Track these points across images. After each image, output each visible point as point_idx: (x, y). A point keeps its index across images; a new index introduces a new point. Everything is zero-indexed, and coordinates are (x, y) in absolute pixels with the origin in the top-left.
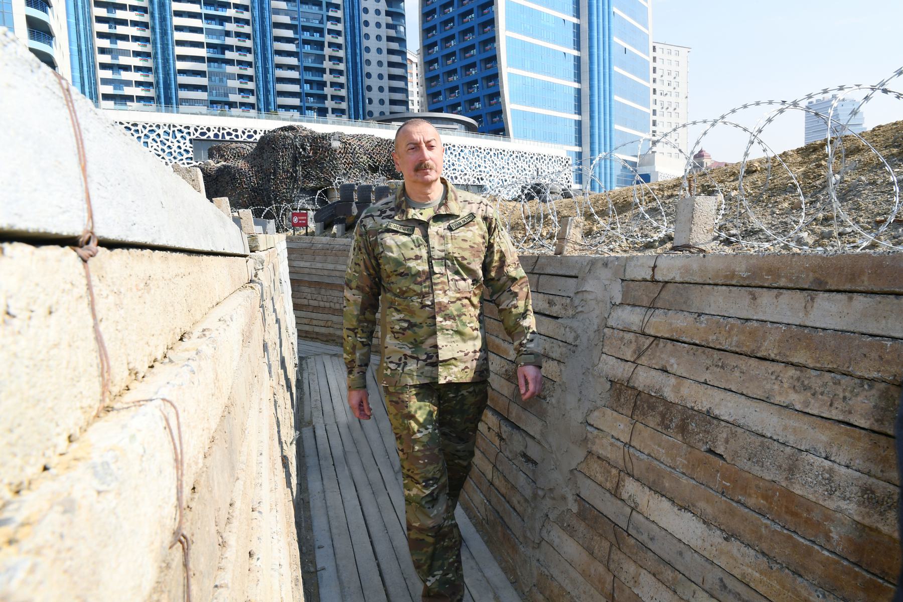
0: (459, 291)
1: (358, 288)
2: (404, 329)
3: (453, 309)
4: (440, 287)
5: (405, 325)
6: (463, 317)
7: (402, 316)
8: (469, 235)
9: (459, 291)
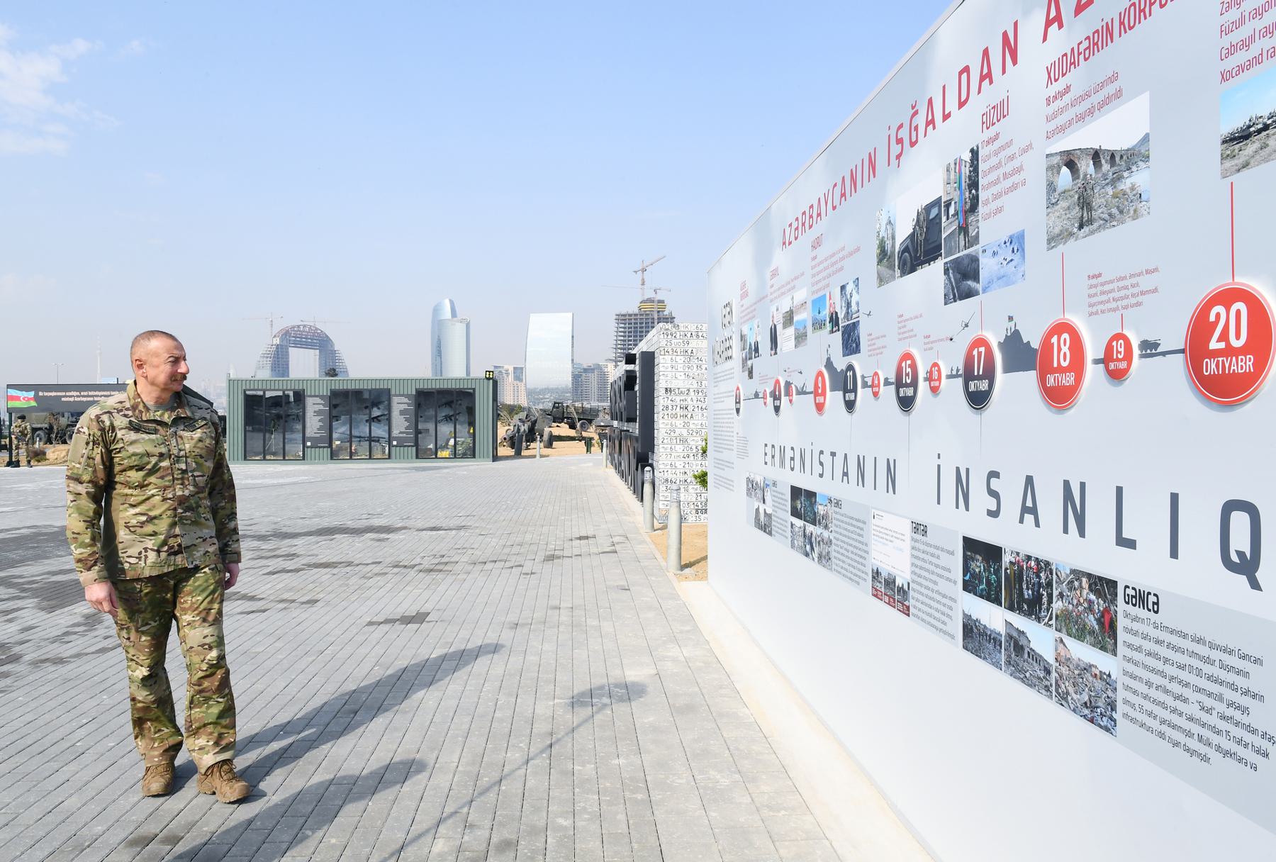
1: (89, 482)
2: (143, 523)
5: (144, 518)
7: (137, 510)
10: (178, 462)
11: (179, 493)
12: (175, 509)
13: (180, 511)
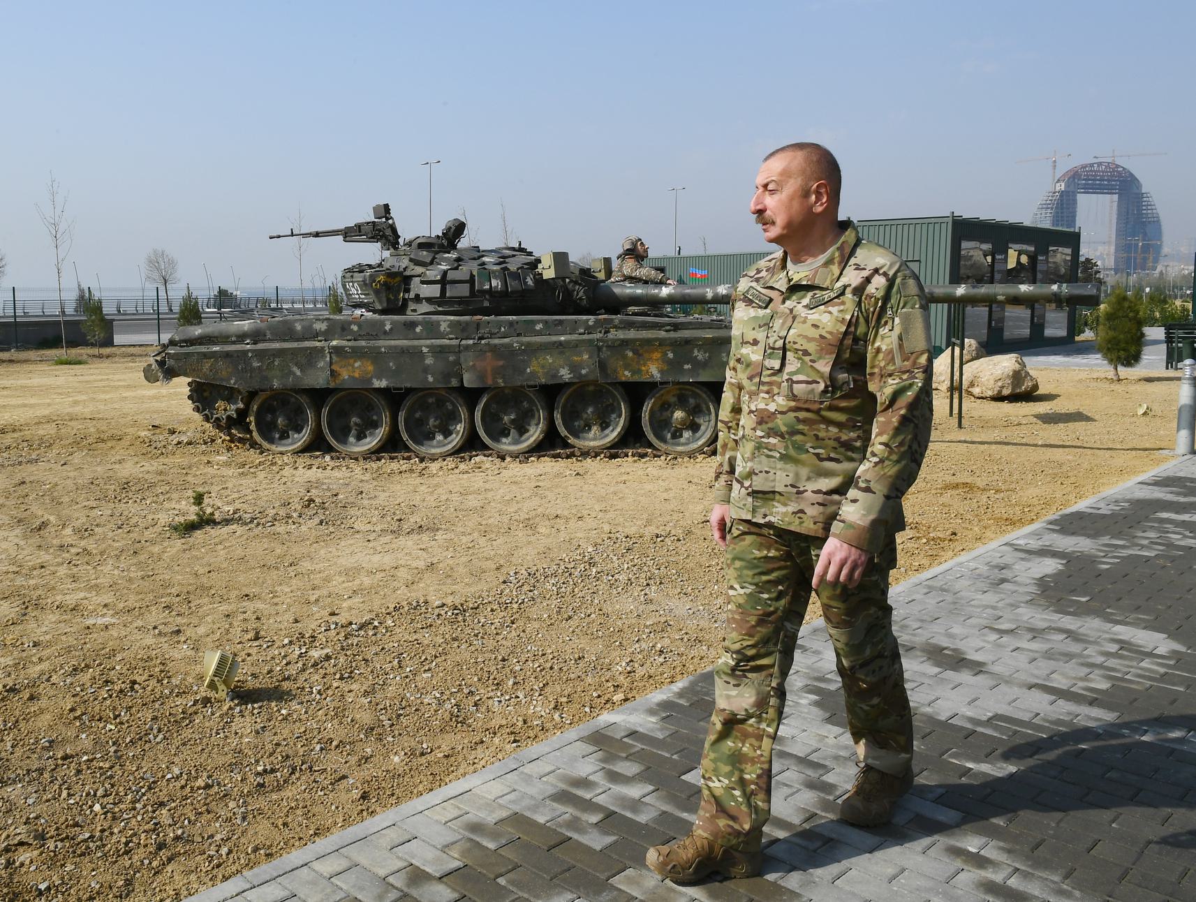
0: (794, 397)
3: (781, 423)
4: (765, 388)
6: (798, 438)
9: (794, 397)
10: (770, 356)
11: (762, 406)
12: (754, 429)
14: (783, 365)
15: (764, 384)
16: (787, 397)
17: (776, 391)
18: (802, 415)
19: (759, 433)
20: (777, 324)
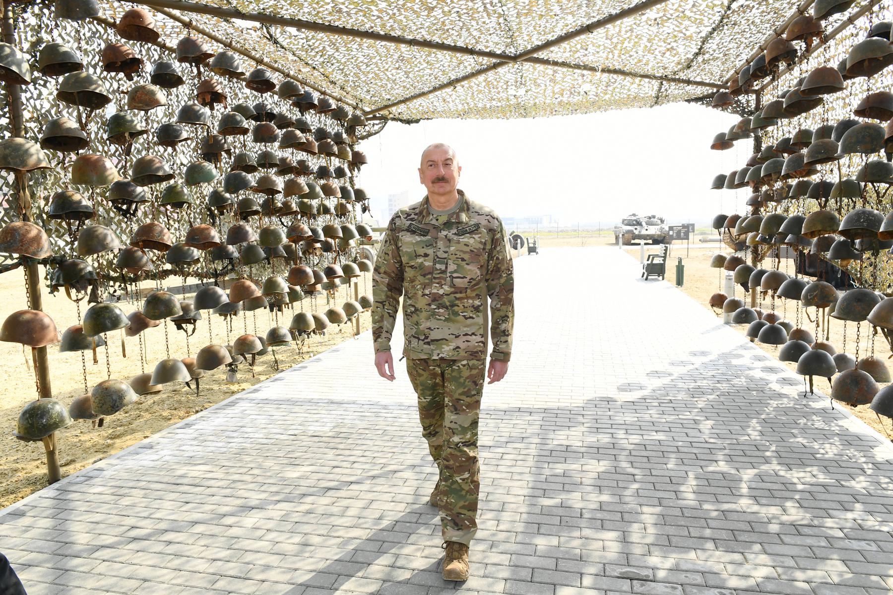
0: (453, 285)
1: (385, 273)
3: (446, 300)
4: (437, 281)
6: (456, 308)
8: (472, 241)
10: (440, 263)
11: (435, 291)
12: (429, 305)
13: (433, 307)
14: (446, 268)
15: (435, 278)
16: (450, 286)
17: (443, 282)
18: (458, 296)
19: (433, 307)
20: (440, 244)
